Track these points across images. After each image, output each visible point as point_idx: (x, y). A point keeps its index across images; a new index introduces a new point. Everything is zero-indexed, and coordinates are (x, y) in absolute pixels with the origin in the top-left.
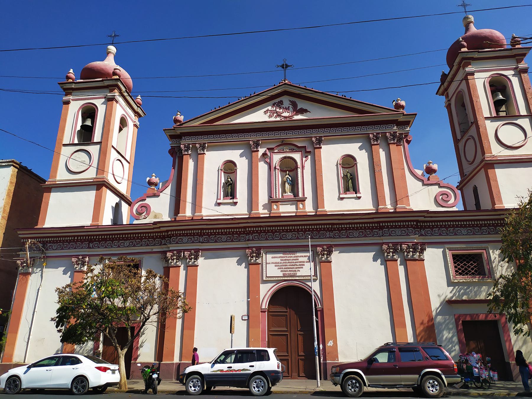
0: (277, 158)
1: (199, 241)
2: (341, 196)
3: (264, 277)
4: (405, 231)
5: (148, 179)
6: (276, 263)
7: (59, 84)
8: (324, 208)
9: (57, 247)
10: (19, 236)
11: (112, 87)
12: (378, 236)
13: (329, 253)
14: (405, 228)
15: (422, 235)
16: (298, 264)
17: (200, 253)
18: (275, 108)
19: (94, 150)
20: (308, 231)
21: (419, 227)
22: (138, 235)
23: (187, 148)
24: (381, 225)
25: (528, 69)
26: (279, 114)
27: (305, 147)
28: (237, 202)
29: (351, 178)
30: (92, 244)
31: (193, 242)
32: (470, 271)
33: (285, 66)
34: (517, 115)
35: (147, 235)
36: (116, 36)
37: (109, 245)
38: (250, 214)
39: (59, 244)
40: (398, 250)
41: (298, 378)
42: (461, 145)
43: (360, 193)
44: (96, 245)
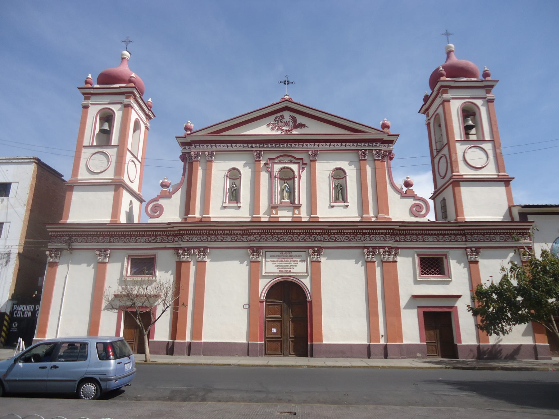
0: (277, 168)
1: (207, 240)
2: (332, 204)
3: (263, 273)
4: (383, 237)
5: (161, 181)
6: (274, 261)
7: (79, 88)
8: (316, 214)
10: (48, 229)
11: (128, 94)
12: (360, 240)
13: (319, 254)
14: (383, 234)
15: (397, 241)
16: (292, 262)
17: (208, 251)
18: (277, 121)
19: (112, 152)
20: (302, 235)
21: (395, 234)
22: (153, 233)
23: (197, 155)
24: (364, 231)
25: (494, 100)
26: (280, 127)
27: (302, 159)
28: (241, 206)
29: (341, 189)
30: (113, 239)
32: (432, 272)
33: (286, 83)
34: (482, 139)
35: (161, 233)
36: (130, 42)
37: (128, 240)
38: (252, 218)
39: (83, 237)
40: (377, 253)
41: (289, 355)
42: (436, 160)
43: (348, 202)
44: (116, 240)
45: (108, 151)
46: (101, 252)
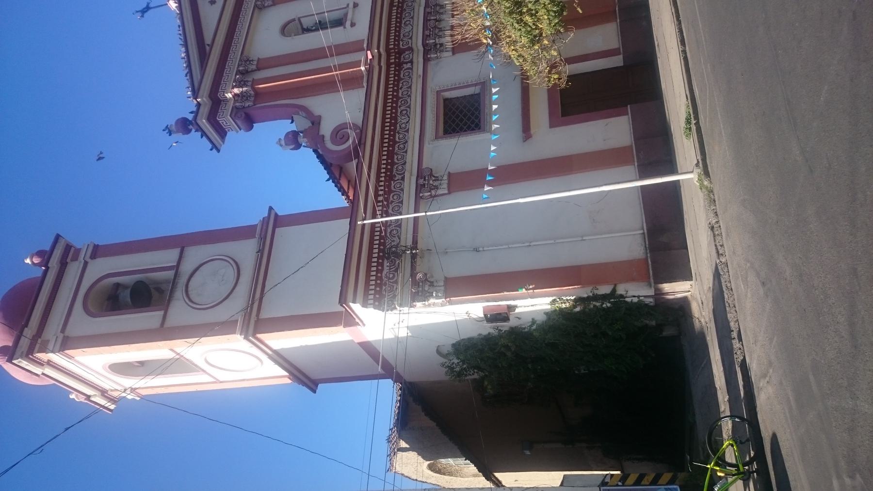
9: (395, 237)
28: (354, 3)
31: (412, 18)
37: (402, 146)
39: (388, 235)
44: (400, 168)
45: (187, 267)
46: (426, 186)
